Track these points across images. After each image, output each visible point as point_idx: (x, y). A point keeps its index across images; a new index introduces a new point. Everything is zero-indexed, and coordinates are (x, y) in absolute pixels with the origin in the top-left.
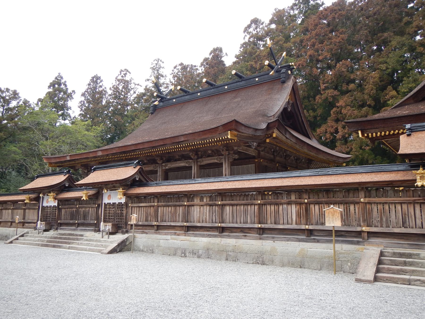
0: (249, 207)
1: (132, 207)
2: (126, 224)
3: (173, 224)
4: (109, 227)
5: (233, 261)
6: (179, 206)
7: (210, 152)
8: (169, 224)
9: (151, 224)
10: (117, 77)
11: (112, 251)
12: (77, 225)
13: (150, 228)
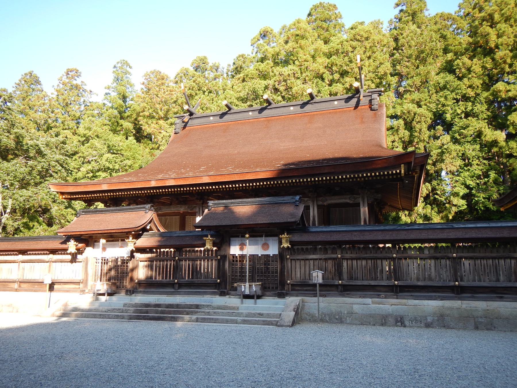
0: (502, 262)
1: (291, 260)
2: (283, 283)
3: (373, 283)
4: (255, 287)
5: (488, 329)
6: (382, 259)
7: (337, 189)
8: (366, 283)
9: (332, 283)
10: (61, 77)
11: (294, 323)
12: (177, 285)
13: (328, 288)
